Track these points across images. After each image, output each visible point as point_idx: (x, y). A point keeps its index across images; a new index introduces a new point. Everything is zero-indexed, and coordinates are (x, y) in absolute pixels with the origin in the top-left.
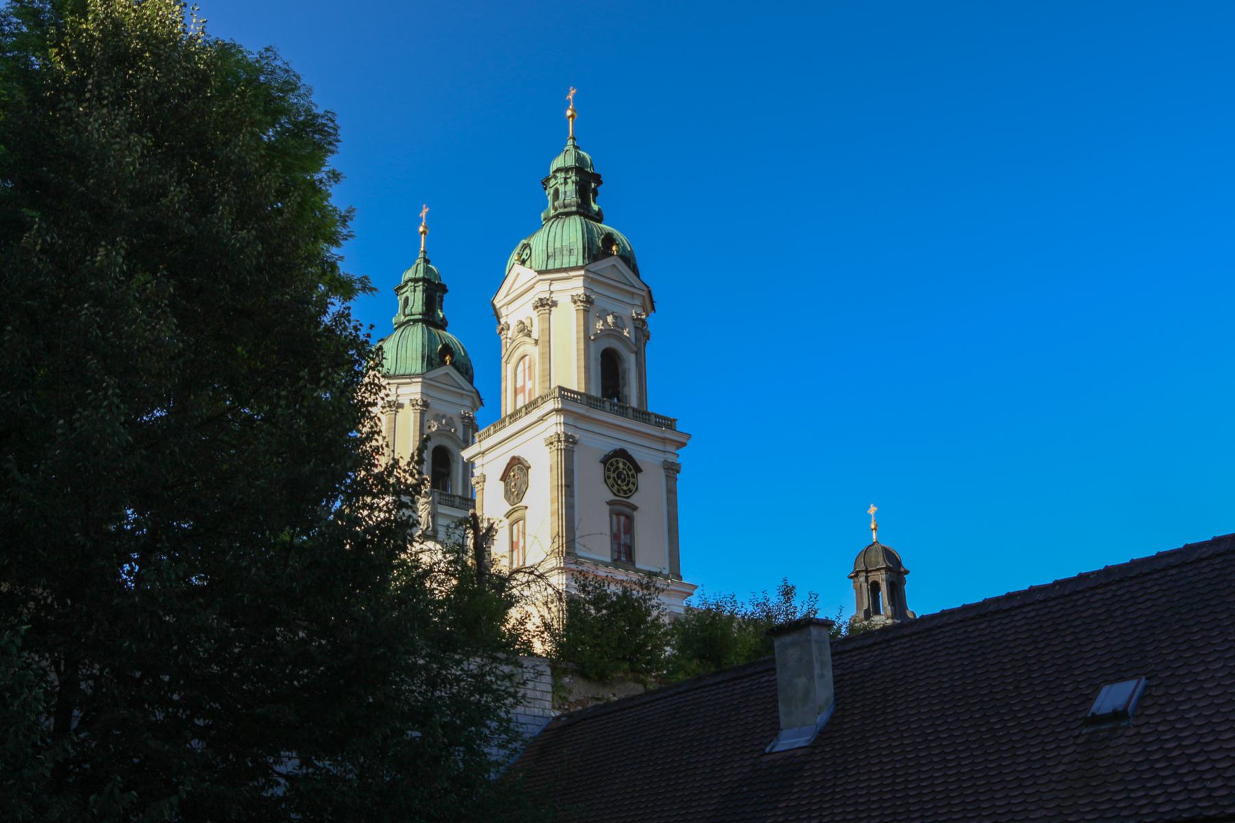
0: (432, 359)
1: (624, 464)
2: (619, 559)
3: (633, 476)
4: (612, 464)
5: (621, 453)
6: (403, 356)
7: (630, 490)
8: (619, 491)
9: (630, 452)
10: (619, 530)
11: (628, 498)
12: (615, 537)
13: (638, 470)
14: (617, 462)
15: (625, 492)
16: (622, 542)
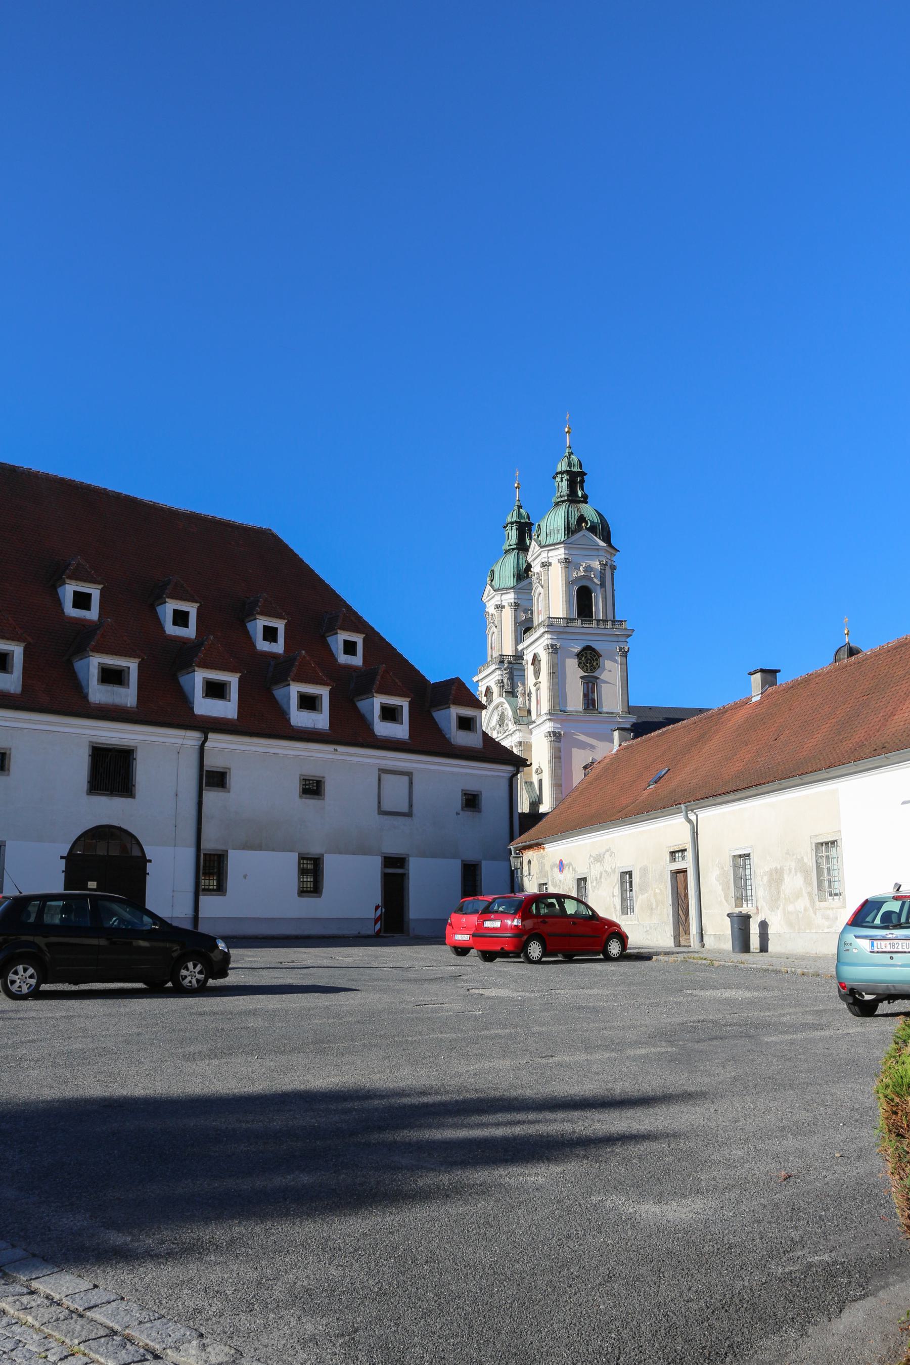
0: (520, 575)
1: (591, 654)
2: (588, 707)
3: (596, 660)
4: (582, 656)
5: (588, 648)
6: (504, 576)
7: (595, 668)
8: (587, 670)
9: (594, 645)
10: (588, 691)
11: (593, 672)
12: (586, 696)
13: (600, 656)
14: (586, 653)
15: (591, 670)
16: (590, 698)
